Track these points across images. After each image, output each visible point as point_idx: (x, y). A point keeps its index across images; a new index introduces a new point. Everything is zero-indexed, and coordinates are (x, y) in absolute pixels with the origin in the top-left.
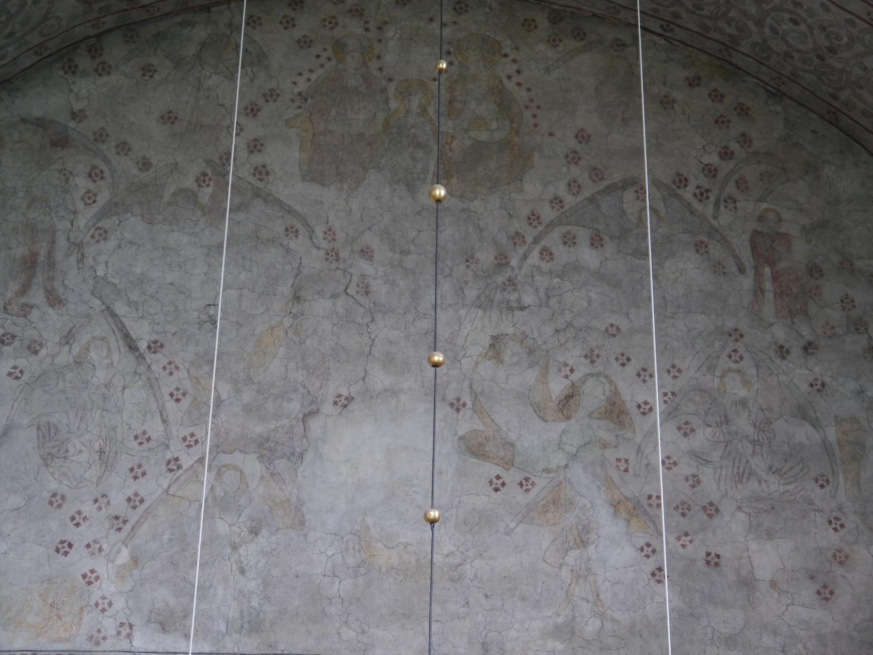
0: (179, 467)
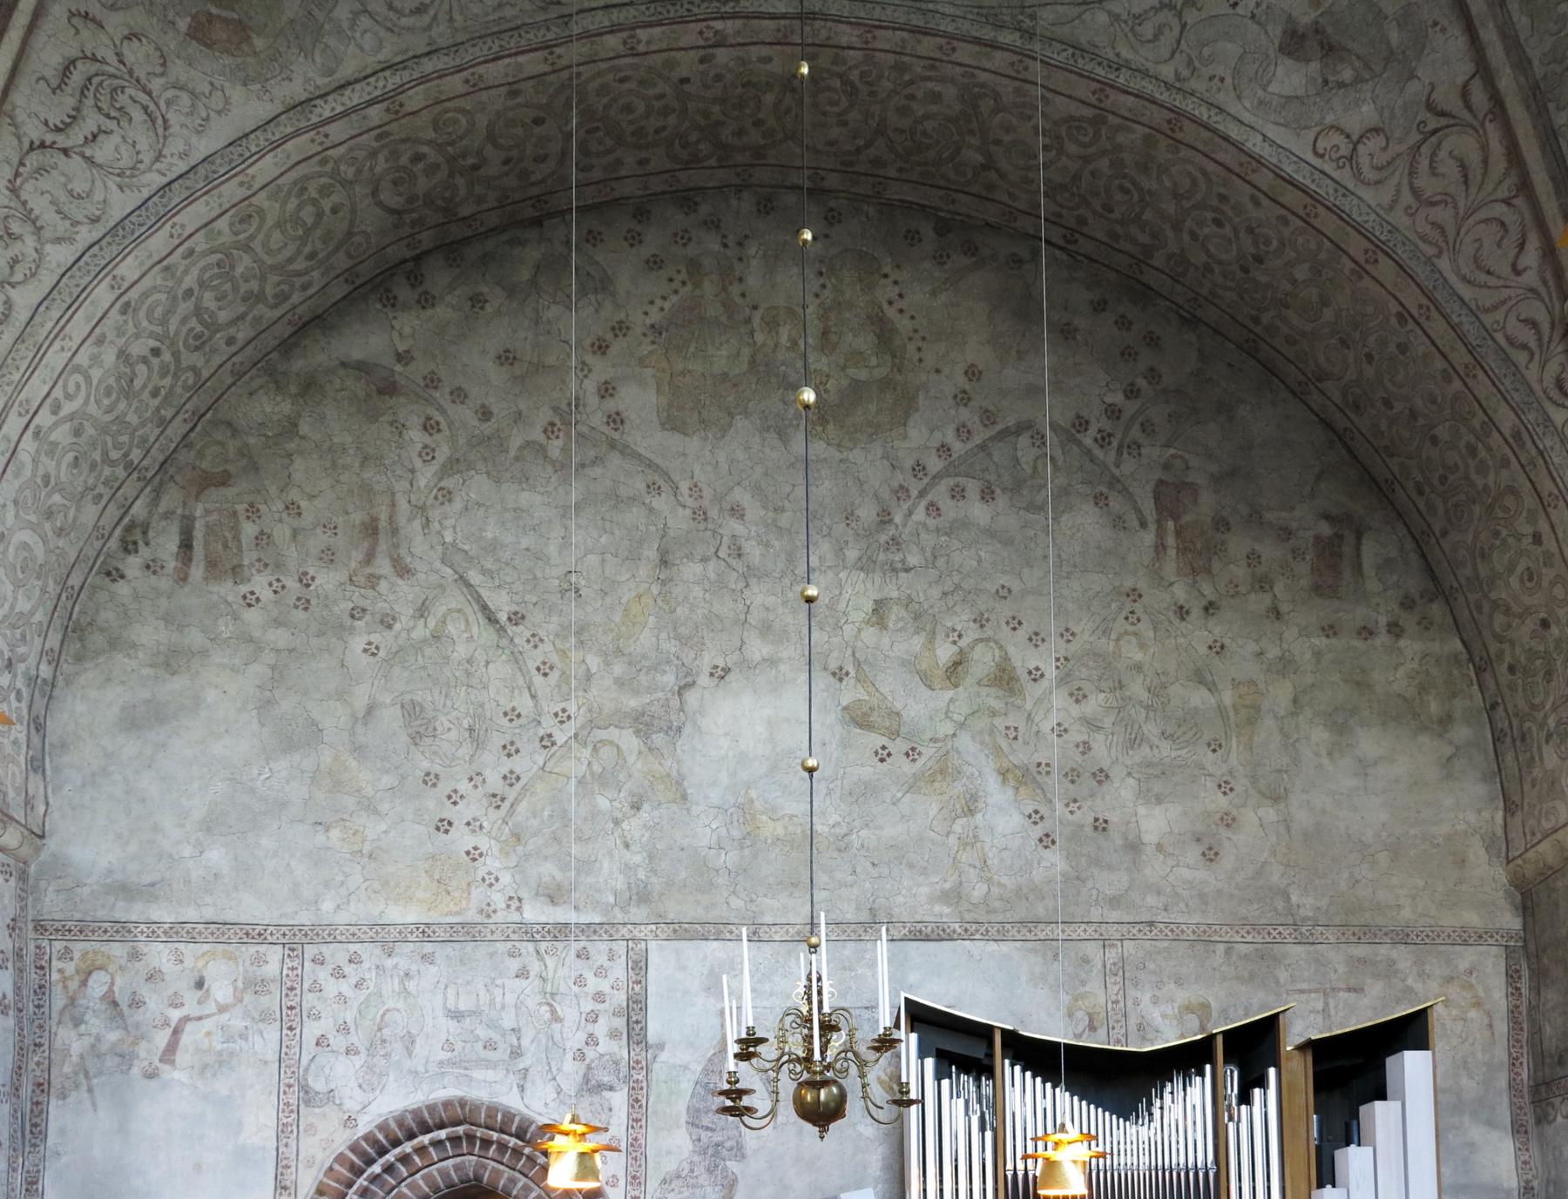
0: (553, 744)
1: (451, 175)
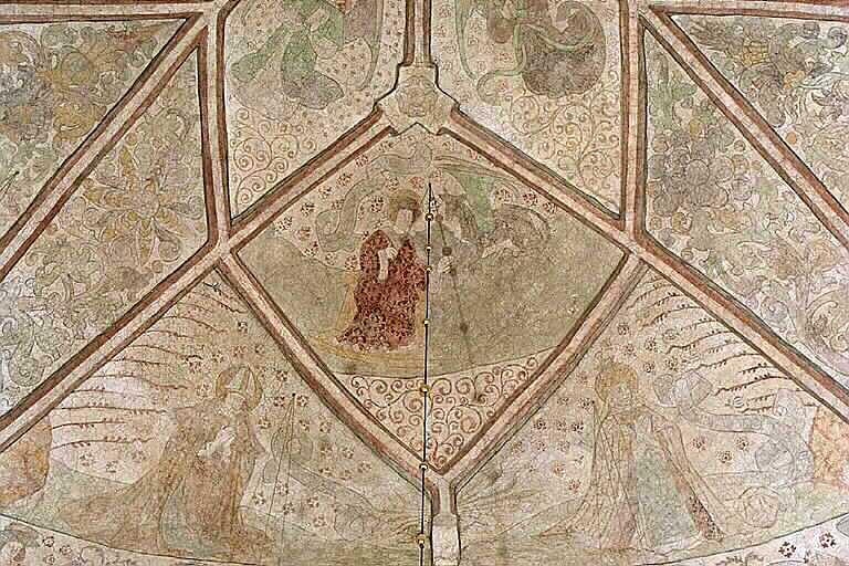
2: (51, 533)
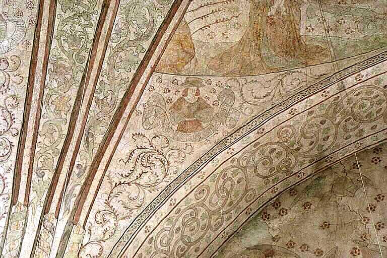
1: (288, 155)
2: (209, 78)
